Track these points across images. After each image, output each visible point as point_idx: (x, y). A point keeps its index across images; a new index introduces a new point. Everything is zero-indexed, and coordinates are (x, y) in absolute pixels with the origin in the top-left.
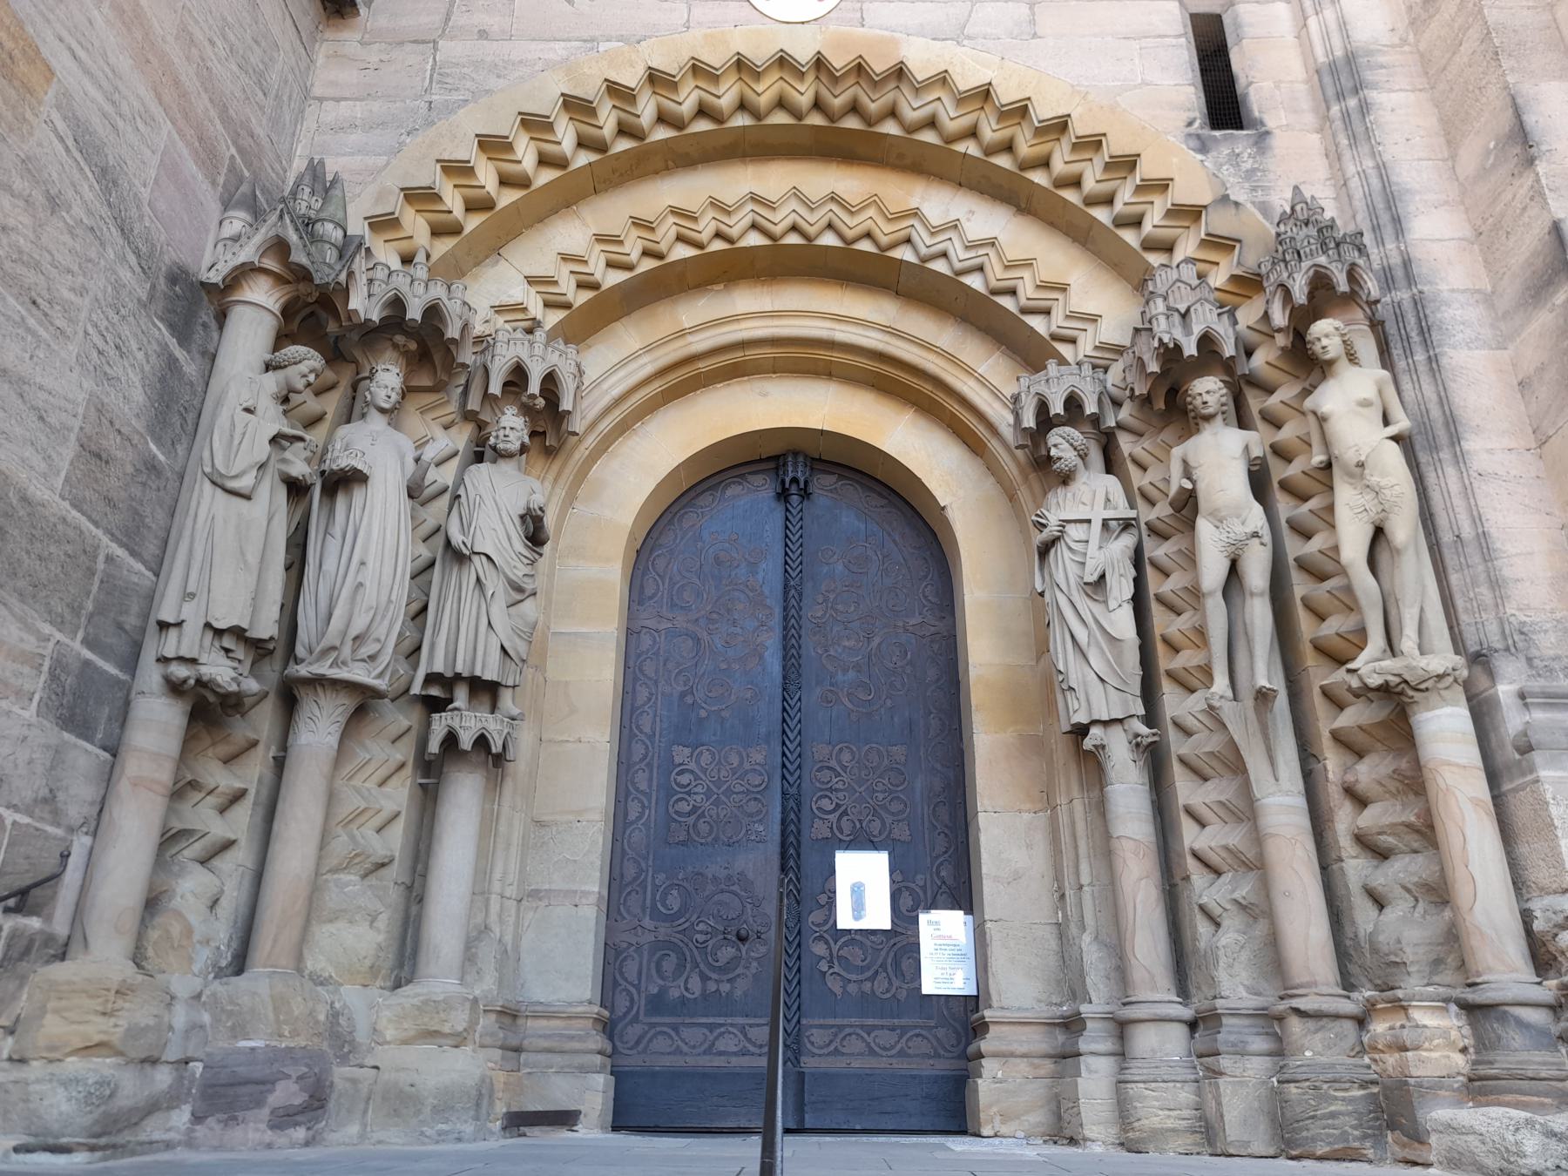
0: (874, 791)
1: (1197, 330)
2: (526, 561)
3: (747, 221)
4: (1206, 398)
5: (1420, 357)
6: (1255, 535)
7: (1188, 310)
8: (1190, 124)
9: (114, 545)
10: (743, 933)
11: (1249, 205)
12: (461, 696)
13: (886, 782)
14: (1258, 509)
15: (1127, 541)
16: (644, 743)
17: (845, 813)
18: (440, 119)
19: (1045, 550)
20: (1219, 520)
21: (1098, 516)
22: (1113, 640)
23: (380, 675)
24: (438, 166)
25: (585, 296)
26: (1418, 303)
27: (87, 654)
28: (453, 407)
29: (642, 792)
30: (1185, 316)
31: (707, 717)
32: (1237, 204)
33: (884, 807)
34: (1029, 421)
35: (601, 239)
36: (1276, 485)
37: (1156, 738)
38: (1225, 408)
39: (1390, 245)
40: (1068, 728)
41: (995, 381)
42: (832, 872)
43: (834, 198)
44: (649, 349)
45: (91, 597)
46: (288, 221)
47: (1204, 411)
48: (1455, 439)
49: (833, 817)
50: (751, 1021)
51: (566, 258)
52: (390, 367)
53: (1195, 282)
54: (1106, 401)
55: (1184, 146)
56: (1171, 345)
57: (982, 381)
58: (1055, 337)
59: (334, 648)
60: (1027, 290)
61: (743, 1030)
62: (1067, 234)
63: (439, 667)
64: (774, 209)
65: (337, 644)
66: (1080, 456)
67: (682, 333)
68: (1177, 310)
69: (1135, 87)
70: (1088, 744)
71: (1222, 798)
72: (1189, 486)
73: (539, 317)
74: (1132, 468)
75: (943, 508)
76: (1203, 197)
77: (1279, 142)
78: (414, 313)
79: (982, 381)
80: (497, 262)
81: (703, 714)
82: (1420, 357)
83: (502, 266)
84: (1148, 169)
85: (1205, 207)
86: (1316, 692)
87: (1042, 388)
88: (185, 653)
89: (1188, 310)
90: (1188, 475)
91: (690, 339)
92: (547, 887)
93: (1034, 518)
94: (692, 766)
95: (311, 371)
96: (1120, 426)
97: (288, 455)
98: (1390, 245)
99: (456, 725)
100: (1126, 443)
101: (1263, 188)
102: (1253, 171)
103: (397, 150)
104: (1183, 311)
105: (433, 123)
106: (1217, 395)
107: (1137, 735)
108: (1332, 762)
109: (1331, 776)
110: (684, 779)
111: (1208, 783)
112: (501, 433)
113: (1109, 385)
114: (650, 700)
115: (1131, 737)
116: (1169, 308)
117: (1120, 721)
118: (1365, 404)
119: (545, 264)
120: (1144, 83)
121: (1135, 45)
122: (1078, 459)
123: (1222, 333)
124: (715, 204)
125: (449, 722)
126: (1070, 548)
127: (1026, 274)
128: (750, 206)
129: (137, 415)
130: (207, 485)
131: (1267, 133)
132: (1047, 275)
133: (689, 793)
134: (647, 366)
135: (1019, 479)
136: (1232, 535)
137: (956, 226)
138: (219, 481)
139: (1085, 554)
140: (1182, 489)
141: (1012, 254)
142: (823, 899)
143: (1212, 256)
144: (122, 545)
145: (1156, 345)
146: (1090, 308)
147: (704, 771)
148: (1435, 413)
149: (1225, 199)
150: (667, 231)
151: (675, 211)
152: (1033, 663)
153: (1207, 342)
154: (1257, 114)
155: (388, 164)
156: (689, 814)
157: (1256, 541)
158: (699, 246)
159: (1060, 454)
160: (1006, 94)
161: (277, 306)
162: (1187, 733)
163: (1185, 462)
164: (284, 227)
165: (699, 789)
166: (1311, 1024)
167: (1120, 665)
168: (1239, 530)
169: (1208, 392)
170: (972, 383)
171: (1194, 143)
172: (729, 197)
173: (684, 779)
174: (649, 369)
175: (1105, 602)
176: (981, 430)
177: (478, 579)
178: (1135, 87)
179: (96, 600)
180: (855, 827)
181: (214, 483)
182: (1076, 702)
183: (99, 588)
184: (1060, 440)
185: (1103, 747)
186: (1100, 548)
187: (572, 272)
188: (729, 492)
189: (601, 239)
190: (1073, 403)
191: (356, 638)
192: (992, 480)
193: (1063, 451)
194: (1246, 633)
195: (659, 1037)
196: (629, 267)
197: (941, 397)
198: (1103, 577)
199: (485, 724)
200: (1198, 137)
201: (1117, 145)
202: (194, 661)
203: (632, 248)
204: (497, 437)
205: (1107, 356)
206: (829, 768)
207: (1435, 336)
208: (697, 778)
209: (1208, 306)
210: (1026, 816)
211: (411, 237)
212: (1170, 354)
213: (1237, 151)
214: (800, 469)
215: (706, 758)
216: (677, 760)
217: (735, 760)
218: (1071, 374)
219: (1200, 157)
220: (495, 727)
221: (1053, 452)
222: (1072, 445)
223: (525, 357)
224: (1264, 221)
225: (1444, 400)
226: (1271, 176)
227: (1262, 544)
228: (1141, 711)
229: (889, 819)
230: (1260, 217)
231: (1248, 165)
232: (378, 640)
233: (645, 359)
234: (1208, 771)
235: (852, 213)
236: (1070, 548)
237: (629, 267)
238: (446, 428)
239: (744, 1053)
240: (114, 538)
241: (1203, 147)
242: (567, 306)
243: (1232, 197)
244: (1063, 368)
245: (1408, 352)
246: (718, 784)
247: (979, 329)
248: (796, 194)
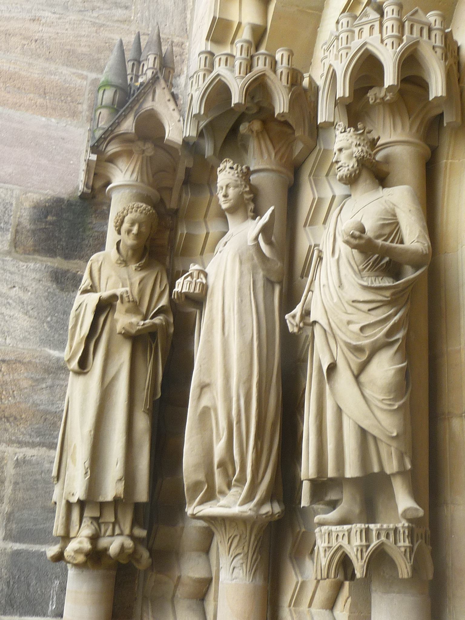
2: (367, 306)
9: (24, 449)
23: (249, 497)
27: (17, 546)
45: (6, 500)
65: (201, 477)
95: (133, 224)
97: (117, 315)
129: (25, 339)
144: (33, 445)
161: (135, 175)
179: (13, 501)
183: (14, 490)
191: (220, 465)
199: (344, 542)
240: (21, 444)
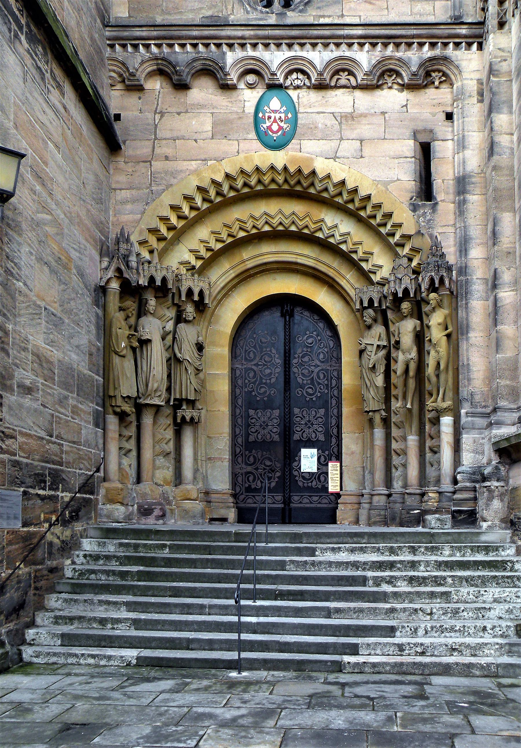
1: (403, 286)
5: (464, 302)
11: (426, 235)
26: (467, 281)
30: (401, 280)
32: (423, 234)
39: (463, 259)
48: (467, 332)
59: (150, 395)
69: (395, 181)
76: (412, 232)
77: (441, 207)
82: (464, 302)
84: (395, 219)
98: (463, 259)
102: (431, 220)
118: (439, 324)
120: (398, 180)
121: (396, 161)
148: (465, 322)
153: (406, 291)
171: (411, 208)
178: (395, 181)
200: (413, 205)
207: (469, 296)
209: (407, 277)
212: (395, 294)
219: (413, 214)
225: (467, 319)
226: (436, 223)
231: (428, 218)
241: (414, 208)
245: (462, 301)
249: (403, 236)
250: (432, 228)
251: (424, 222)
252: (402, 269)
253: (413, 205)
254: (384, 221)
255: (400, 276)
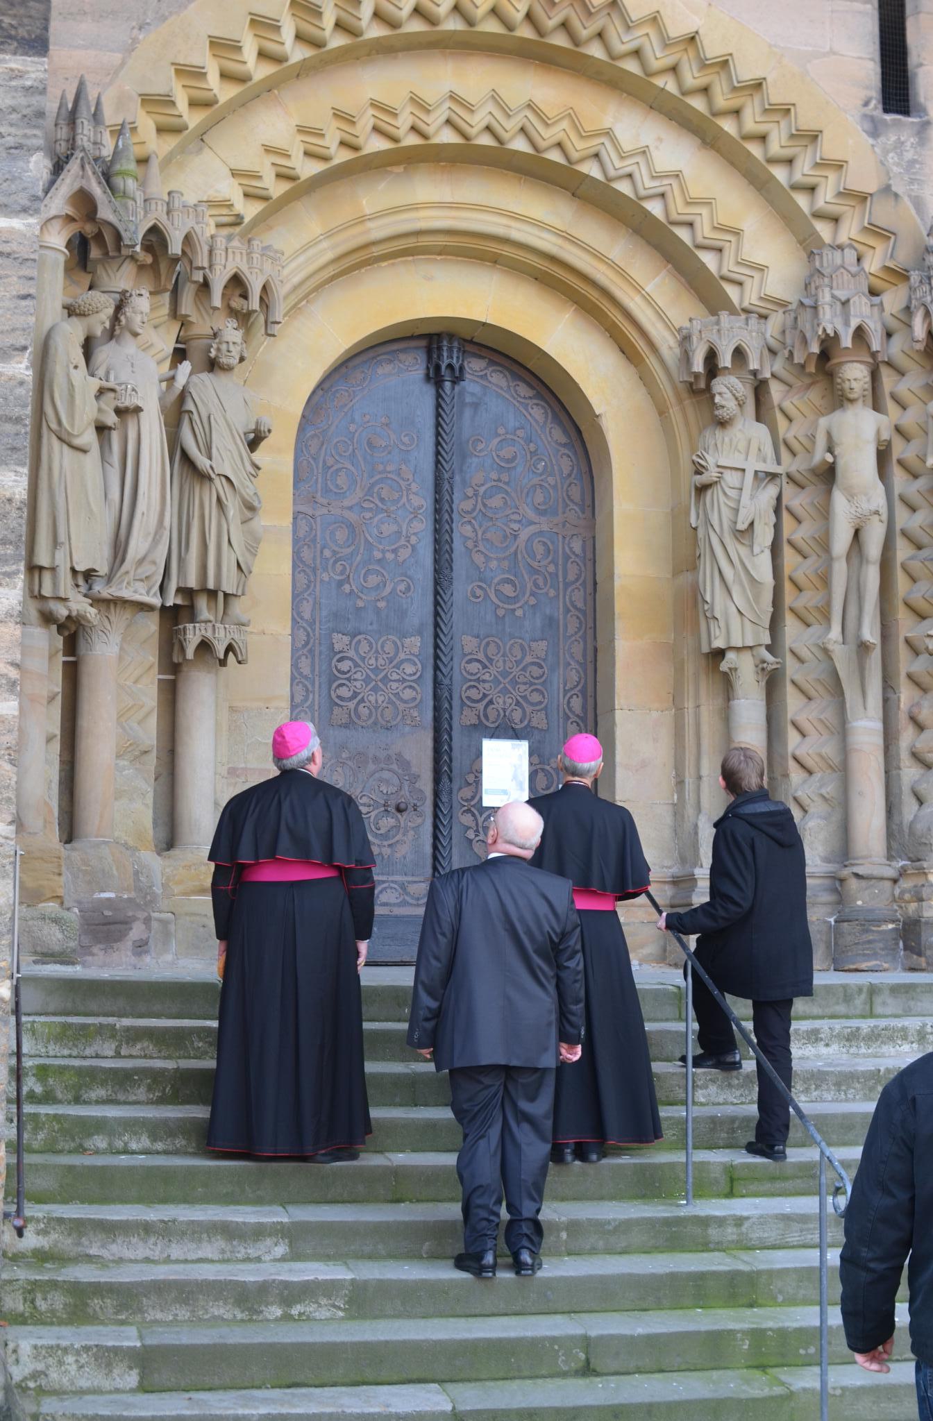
0: (517, 683)
1: (854, 323)
3: (443, 118)
4: (854, 385)
6: (877, 513)
7: (848, 301)
8: (866, 104)
10: (403, 806)
11: (906, 199)
12: (202, 603)
13: (527, 675)
14: (880, 487)
15: (771, 491)
16: (305, 630)
17: (491, 702)
18: (171, 13)
19: (702, 489)
20: (851, 496)
21: (753, 465)
22: (753, 580)
24: (173, 69)
25: (285, 187)
28: (165, 310)
29: (306, 677)
30: (845, 303)
31: (364, 607)
32: (896, 195)
33: (524, 698)
34: (698, 366)
35: (302, 130)
36: (894, 461)
37: (778, 666)
38: (866, 393)
40: (705, 649)
41: (661, 302)
42: (479, 754)
43: (530, 106)
44: (329, 234)
46: (90, 173)
47: (852, 396)
49: (481, 706)
50: (410, 879)
51: (269, 150)
52: (143, 292)
53: (854, 269)
54: (766, 352)
55: (859, 128)
56: (832, 334)
57: (648, 299)
58: (723, 278)
60: (705, 230)
61: (403, 886)
62: (744, 176)
63: (192, 583)
64: (472, 111)
66: (739, 405)
67: (362, 220)
68: (840, 300)
70: (724, 666)
71: (822, 717)
72: (830, 459)
73: (242, 212)
74: (779, 417)
75: (597, 416)
76: (871, 186)
78: (175, 248)
79: (648, 299)
80: (200, 150)
81: (360, 604)
83: (207, 155)
85: (871, 195)
86: (901, 640)
87: (714, 338)
88: (62, 595)
89: (848, 301)
90: (830, 450)
91: (370, 225)
92: (243, 765)
93: (694, 458)
94: (351, 653)
96: (773, 375)
99: (209, 634)
100: (776, 390)
101: (920, 182)
102: (912, 163)
103: (130, 49)
104: (843, 299)
105: (164, 19)
106: (862, 383)
107: (764, 662)
108: (906, 695)
109: (902, 705)
110: (345, 666)
111: (812, 702)
112: (224, 347)
113: (768, 336)
114: (308, 587)
115: (758, 662)
116: (833, 296)
117: (751, 648)
119: (252, 158)
120: (832, 52)
122: (738, 408)
123: (873, 328)
124: (415, 101)
125: (203, 632)
126: (725, 494)
127: (704, 211)
128: (448, 104)
130: (56, 443)
131: (928, 123)
132: (723, 219)
133: (349, 679)
134: (326, 252)
135: (673, 400)
136: (859, 510)
137: (644, 152)
138: (64, 436)
139: (739, 501)
140: (825, 461)
141: (695, 191)
142: (471, 778)
143: (871, 242)
145: (820, 333)
146: (759, 258)
147: (363, 659)
149: (887, 190)
150: (367, 121)
151: (375, 105)
152: (669, 576)
154: (922, 99)
155: (123, 64)
156: (351, 699)
157: (876, 517)
158: (395, 140)
159: (724, 403)
160: (713, 48)
162: (800, 660)
163: (829, 435)
164: (88, 180)
165: (358, 676)
166: (864, 883)
167: (757, 602)
168: (866, 506)
169: (855, 380)
170: (638, 299)
171: (867, 126)
172: (430, 94)
173: (345, 666)
174: (330, 255)
175: (751, 547)
176: (641, 345)
177: (219, 500)
180: (499, 715)
181: (60, 438)
182: (717, 630)
184: (725, 390)
185: (736, 669)
186: (752, 497)
187: (273, 164)
188: (380, 371)
189: (302, 130)
190: (739, 353)
192: (643, 390)
193: (725, 400)
194: (859, 589)
195: (389, 891)
196: (325, 159)
197: (606, 306)
198: (752, 524)
200: (872, 119)
201: (806, 119)
202: (65, 600)
203: (331, 142)
204: (218, 350)
205: (769, 306)
206: (479, 661)
208: (356, 665)
210: (655, 714)
211: (144, 143)
213: (902, 139)
214: (455, 355)
215: (364, 647)
216: (337, 647)
217: (389, 647)
218: (740, 328)
219: (871, 141)
220: (235, 635)
221: (717, 399)
222: (734, 395)
223: (244, 268)
224: (916, 216)
227: (881, 521)
228: (768, 641)
229: (529, 709)
230: (913, 212)
231: (909, 155)
232: (154, 563)
233: (325, 244)
234: (813, 693)
235: (547, 125)
236: (725, 494)
237: (325, 159)
238: (155, 327)
239: (404, 903)
241: (875, 130)
242: (266, 199)
243: (894, 189)
244: (732, 317)
246: (376, 670)
247: (649, 242)
248: (495, 98)
249: (845, 194)
250: (920, 182)
251: (898, 165)
252: (846, 276)
253: (872, 119)
254: (787, 153)
255: (843, 295)
